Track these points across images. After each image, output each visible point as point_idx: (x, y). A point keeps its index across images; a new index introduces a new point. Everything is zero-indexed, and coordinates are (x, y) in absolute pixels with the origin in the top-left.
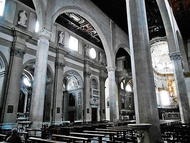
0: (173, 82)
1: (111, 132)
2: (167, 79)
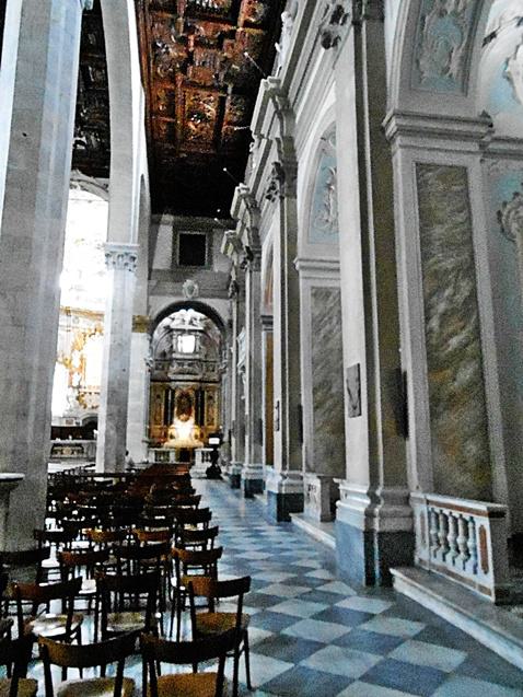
1: (377, 464)
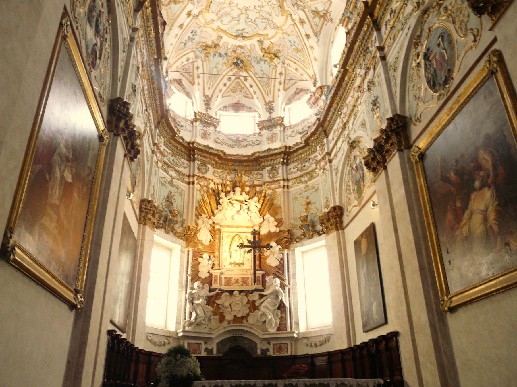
0: (224, 200)
2: (196, 172)
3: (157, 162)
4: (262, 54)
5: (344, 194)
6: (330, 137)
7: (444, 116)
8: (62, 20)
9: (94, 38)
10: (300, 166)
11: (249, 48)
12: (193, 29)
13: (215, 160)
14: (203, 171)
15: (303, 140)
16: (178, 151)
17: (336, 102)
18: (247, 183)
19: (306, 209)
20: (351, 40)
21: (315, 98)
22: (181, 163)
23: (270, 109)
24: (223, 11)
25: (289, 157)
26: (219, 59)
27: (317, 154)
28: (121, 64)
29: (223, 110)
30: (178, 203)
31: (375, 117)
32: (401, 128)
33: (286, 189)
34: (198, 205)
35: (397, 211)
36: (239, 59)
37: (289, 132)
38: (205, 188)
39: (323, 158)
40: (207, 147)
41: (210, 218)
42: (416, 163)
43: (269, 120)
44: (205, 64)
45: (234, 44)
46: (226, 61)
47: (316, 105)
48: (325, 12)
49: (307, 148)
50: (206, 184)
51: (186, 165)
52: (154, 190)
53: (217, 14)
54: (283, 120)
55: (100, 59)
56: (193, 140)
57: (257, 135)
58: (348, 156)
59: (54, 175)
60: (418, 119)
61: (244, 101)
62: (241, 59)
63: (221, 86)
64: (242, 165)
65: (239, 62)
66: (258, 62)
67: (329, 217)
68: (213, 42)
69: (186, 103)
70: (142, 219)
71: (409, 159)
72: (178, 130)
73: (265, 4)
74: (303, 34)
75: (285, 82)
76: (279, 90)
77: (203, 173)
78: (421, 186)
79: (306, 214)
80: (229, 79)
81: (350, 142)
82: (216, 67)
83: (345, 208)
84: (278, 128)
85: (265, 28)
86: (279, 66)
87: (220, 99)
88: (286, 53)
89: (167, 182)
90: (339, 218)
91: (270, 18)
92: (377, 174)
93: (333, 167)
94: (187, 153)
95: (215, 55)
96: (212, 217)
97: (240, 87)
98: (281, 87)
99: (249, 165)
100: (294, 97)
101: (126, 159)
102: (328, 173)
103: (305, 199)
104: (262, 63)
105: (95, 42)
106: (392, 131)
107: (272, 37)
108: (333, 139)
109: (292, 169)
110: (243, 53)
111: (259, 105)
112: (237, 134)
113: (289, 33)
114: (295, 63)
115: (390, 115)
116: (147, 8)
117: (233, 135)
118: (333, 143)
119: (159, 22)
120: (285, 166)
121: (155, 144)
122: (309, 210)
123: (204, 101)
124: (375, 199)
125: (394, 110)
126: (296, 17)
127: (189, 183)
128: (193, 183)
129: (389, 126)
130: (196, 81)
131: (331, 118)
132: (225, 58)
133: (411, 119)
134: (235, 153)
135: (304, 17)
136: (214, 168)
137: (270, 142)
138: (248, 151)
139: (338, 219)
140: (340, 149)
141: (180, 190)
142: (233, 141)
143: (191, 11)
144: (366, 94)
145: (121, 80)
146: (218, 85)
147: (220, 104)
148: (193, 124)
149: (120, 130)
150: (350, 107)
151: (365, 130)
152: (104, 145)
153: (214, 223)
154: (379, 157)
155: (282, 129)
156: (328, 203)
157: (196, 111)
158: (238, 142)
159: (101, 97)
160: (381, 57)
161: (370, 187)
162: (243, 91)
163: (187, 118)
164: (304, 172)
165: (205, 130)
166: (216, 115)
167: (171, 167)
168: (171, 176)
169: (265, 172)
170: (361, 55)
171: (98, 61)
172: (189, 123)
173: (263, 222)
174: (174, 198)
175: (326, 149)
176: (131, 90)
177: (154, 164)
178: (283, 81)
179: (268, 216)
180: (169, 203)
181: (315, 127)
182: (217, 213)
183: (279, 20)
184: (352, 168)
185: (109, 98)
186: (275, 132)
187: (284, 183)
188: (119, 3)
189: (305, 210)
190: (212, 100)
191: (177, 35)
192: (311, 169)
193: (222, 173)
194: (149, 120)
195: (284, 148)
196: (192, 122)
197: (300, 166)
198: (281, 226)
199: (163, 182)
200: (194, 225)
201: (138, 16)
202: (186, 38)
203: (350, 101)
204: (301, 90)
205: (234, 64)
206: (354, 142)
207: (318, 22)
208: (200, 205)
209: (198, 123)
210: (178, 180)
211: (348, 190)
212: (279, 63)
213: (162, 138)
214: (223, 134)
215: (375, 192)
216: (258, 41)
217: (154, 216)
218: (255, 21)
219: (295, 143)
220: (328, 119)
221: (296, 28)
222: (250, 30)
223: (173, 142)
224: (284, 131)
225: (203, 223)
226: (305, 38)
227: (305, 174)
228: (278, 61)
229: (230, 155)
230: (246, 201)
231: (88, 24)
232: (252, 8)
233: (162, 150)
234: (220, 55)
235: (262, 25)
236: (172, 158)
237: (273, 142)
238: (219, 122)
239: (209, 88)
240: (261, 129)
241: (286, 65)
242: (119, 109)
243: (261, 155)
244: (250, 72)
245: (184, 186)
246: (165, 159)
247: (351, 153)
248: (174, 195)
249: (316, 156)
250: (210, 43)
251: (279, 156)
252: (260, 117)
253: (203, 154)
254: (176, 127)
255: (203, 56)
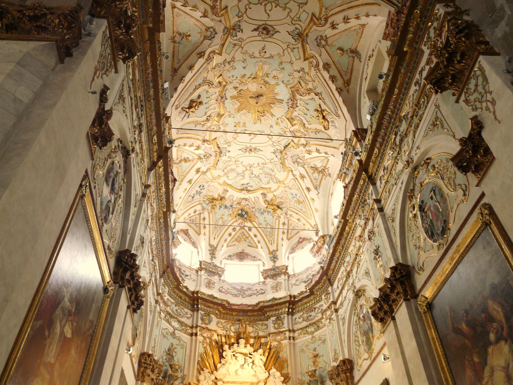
0: (228, 353)
2: (200, 323)
3: (160, 313)
4: (266, 206)
5: (353, 346)
6: (335, 286)
7: (446, 266)
8: (82, 182)
9: (109, 195)
10: (305, 315)
11: (253, 200)
12: (201, 184)
13: (219, 310)
14: (207, 322)
15: (308, 289)
16: (182, 301)
17: (338, 250)
18: (252, 335)
19: (314, 363)
20: (348, 193)
21: (318, 247)
22: (184, 313)
23: (274, 258)
24: (230, 168)
25: (294, 307)
26: (224, 211)
27: (322, 303)
28: (132, 217)
29: (227, 259)
30: (179, 357)
31: (378, 266)
32: (405, 277)
33: (292, 341)
34: (200, 359)
35: (411, 366)
36: (244, 210)
37: (293, 281)
38: (208, 340)
39: (329, 307)
40: (211, 296)
41: (212, 373)
42: (425, 313)
43: (273, 269)
44: (211, 215)
45: (239, 197)
46: (231, 212)
47: (319, 253)
48: (323, 168)
49: (312, 297)
50: (209, 336)
51: (189, 316)
52: (155, 343)
53: (223, 170)
54: (287, 269)
55: (112, 213)
56: (197, 290)
57: (261, 284)
58: (354, 305)
59: (54, 330)
60: (421, 268)
61: (248, 250)
62: (246, 210)
63: (226, 236)
64: (246, 315)
65: (244, 213)
66: (262, 213)
67: (338, 372)
68: (219, 195)
69: (192, 252)
70: (141, 375)
71: (417, 309)
72: (183, 280)
73: (267, 161)
74: (304, 187)
75: (288, 232)
76: (283, 239)
77: (206, 324)
78: (433, 339)
79: (313, 368)
80: (234, 229)
81: (355, 291)
82: (221, 218)
83: (355, 361)
84: (283, 276)
85: (268, 183)
86: (282, 217)
87: (225, 248)
88: (288, 205)
89: (169, 334)
90: (349, 373)
91: (273, 174)
92: (385, 324)
93: (340, 317)
94: (191, 302)
95: (221, 207)
96: (215, 372)
97: (244, 237)
98: (285, 236)
99: (253, 315)
100: (297, 245)
101: (129, 310)
102: (335, 323)
103: (312, 351)
104: (266, 214)
105: (110, 198)
106: (396, 280)
107: (275, 191)
108: (338, 287)
109: (297, 319)
110: (247, 205)
111: (263, 254)
112: (242, 283)
113: (291, 186)
114: (297, 214)
115: (393, 264)
116: (160, 167)
117: (237, 284)
118: (338, 291)
119: (170, 179)
120: (290, 316)
121: (159, 294)
122: (317, 364)
123: (209, 250)
124: (386, 351)
125: (396, 259)
126: (296, 173)
127: (192, 335)
128: (196, 334)
129: (393, 275)
130: (203, 231)
131: (335, 266)
132: (230, 210)
133: (414, 267)
134: (239, 303)
135: (303, 172)
136: (217, 318)
137: (274, 291)
138: (252, 301)
139: (348, 374)
140: (345, 298)
141: (182, 342)
142: (238, 290)
143: (199, 168)
144: (368, 243)
145: (130, 232)
146: (223, 235)
147: (225, 253)
148: (197, 273)
149: (126, 281)
150: (353, 256)
151: (369, 278)
152: (108, 297)
153: (216, 378)
154: (386, 307)
155: (287, 277)
156: (337, 356)
157: (201, 260)
158: (242, 291)
159: (109, 249)
160: (378, 208)
161: (379, 339)
162: (248, 240)
163: (192, 267)
164: (310, 322)
165: (210, 280)
166: (221, 264)
167: (174, 317)
168: (173, 327)
169: (270, 322)
170: (360, 207)
171: (111, 216)
172: (194, 272)
173: (269, 377)
174: (175, 350)
175: (331, 298)
176: (139, 242)
177: (157, 315)
178: (286, 231)
179: (273, 370)
180: (169, 356)
181: (319, 275)
182: (220, 367)
183: (281, 175)
184: (359, 318)
185: (118, 250)
186: (279, 281)
187: (289, 334)
188: (135, 164)
189: (312, 364)
190: (217, 249)
191: (186, 189)
192: (317, 319)
193: (226, 324)
194: (155, 270)
195: (289, 297)
196: (197, 272)
197: (305, 315)
198: (288, 381)
199: (165, 334)
200: (195, 381)
201: (151, 174)
202: (194, 192)
203: (352, 249)
204: (304, 239)
205: (239, 215)
206: (359, 290)
207: (317, 177)
208: (202, 359)
209: (203, 272)
210: (180, 331)
211: (357, 341)
212: (282, 214)
213: (166, 287)
214: (228, 283)
215: (385, 344)
216: (262, 194)
217: (153, 371)
218: (259, 176)
219: (299, 292)
220: (331, 267)
221: (297, 182)
222: (254, 184)
223: (177, 292)
224: (288, 280)
225: (205, 379)
226: (305, 191)
227: (311, 325)
228: (281, 212)
229: (234, 305)
230: (250, 354)
231: (105, 183)
232: (256, 165)
233: (166, 300)
234: (226, 207)
235: (265, 180)
236: (175, 308)
237: (277, 291)
238: (224, 271)
239: (215, 238)
240: (265, 278)
241: (288, 216)
242: (127, 260)
243: (266, 304)
244: (254, 223)
245: (186, 338)
246: (168, 309)
247: (357, 302)
248: (176, 348)
249: (322, 305)
250: (216, 196)
251: (284, 305)
252: (264, 266)
253: (207, 304)
254: (181, 276)
255: (209, 208)
